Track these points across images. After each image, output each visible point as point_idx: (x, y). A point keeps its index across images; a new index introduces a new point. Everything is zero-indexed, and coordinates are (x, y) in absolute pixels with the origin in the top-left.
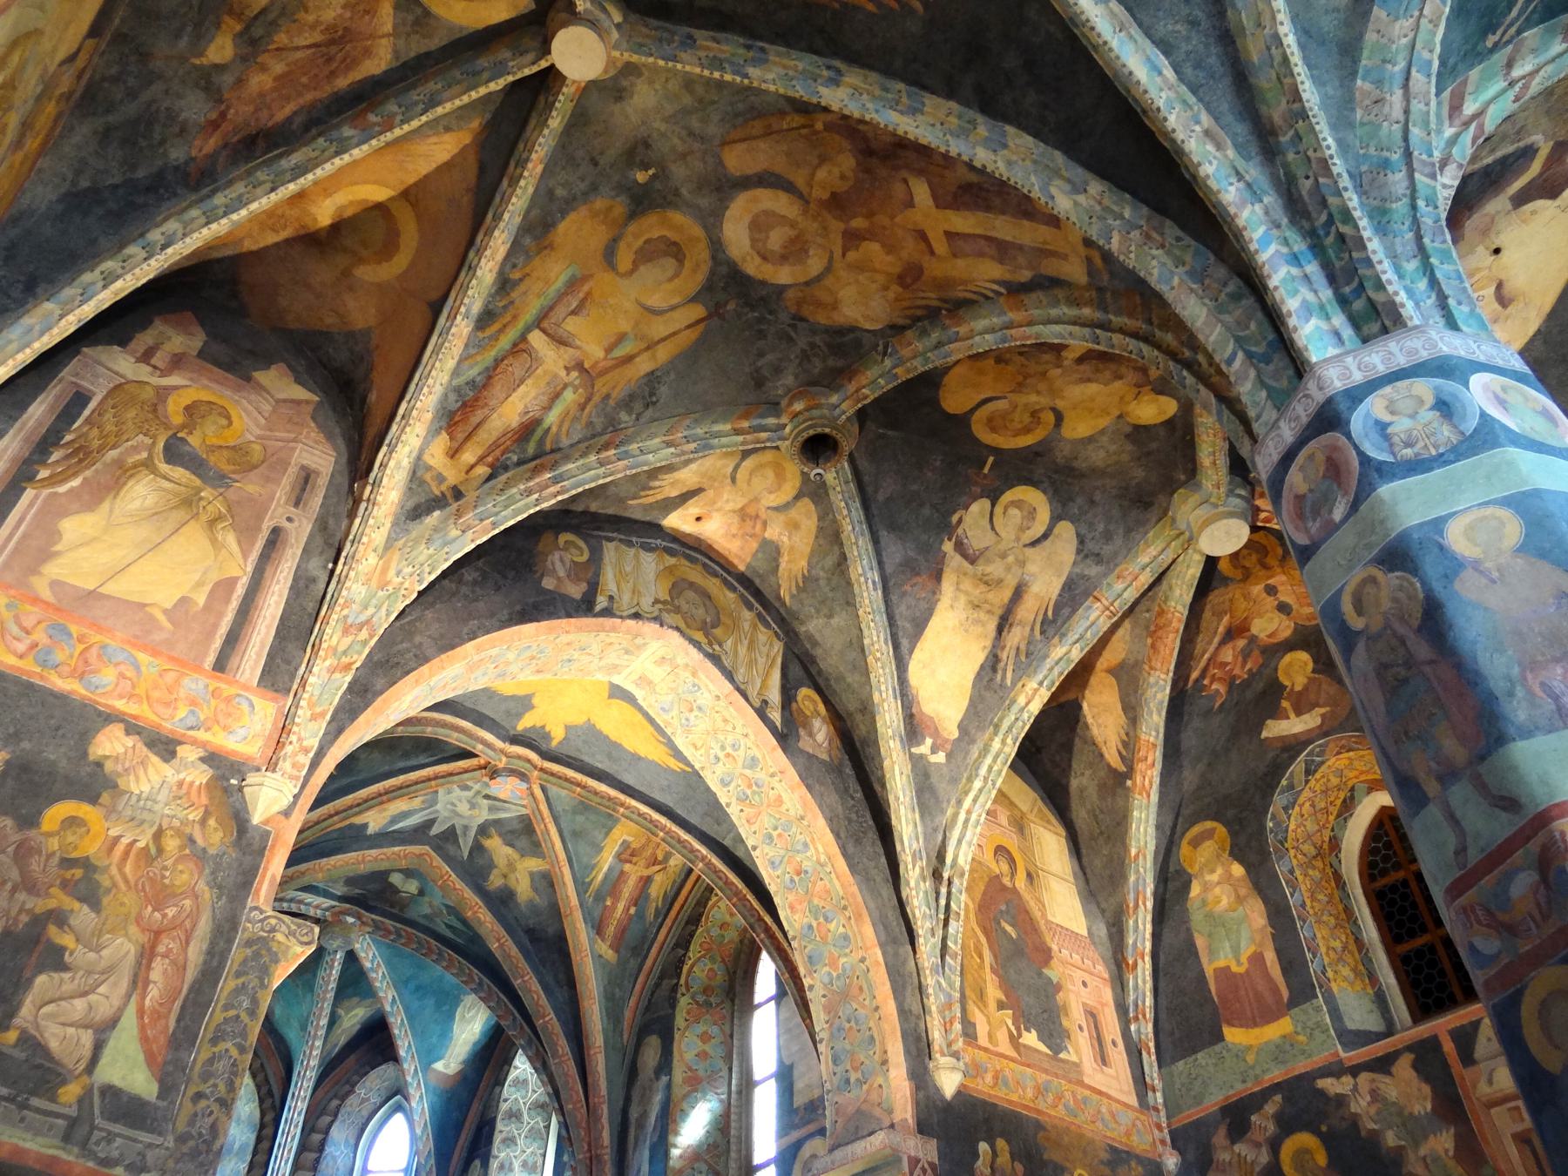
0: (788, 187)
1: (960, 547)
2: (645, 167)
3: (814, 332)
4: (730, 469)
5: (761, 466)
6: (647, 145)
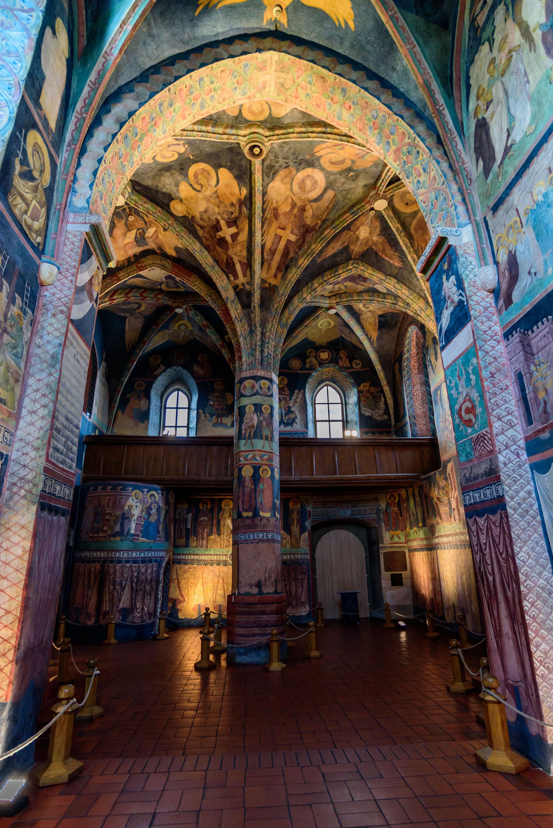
0: (316, 200)
1: (178, 144)
2: (352, 176)
3: (281, 166)
4: (272, 108)
5: (262, 111)
6: (354, 180)
